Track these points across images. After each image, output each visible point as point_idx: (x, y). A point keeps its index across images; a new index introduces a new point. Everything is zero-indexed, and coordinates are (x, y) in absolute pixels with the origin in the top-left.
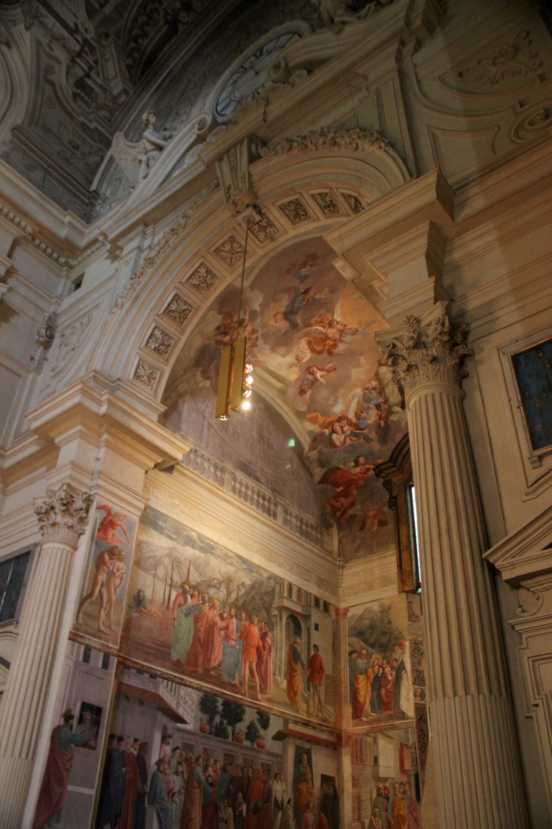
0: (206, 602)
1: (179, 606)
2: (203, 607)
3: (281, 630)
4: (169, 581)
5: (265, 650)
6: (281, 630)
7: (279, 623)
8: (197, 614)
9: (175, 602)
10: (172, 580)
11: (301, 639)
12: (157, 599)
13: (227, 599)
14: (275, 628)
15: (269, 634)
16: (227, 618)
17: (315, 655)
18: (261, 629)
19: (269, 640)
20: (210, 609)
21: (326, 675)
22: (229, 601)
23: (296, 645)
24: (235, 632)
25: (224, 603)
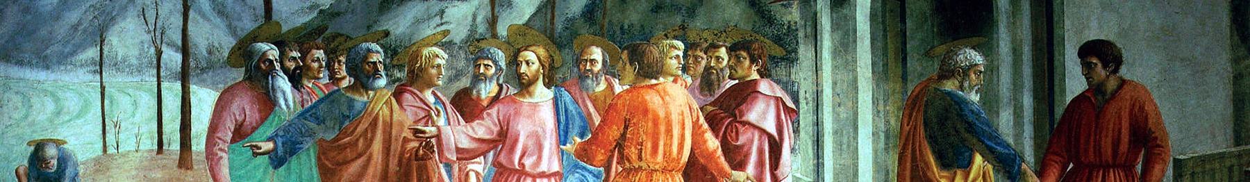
0: (375, 74)
1: (240, 134)
2: (361, 99)
3: (846, 44)
4: (173, 58)
5: (740, 166)
6: (846, 44)
7: (825, 22)
8: (330, 136)
9: (213, 128)
10: (185, 50)
11: (987, 48)
12: (128, 145)
13: (493, 22)
14: (805, 52)
15: (764, 87)
16: (495, 100)
17: (1096, 89)
18: (707, 82)
19: (762, 114)
20: (398, 95)
21: (1177, 164)
22: (502, 30)
23: (950, 86)
24: (549, 143)
25: (475, 47)
